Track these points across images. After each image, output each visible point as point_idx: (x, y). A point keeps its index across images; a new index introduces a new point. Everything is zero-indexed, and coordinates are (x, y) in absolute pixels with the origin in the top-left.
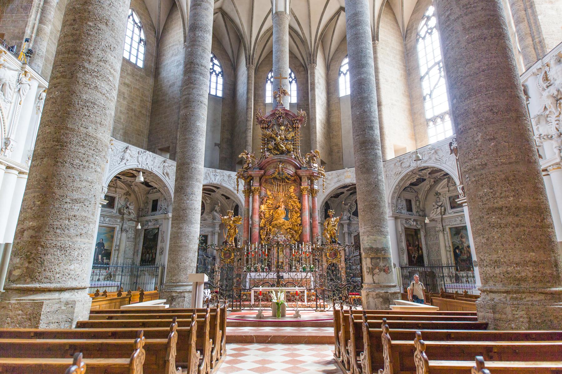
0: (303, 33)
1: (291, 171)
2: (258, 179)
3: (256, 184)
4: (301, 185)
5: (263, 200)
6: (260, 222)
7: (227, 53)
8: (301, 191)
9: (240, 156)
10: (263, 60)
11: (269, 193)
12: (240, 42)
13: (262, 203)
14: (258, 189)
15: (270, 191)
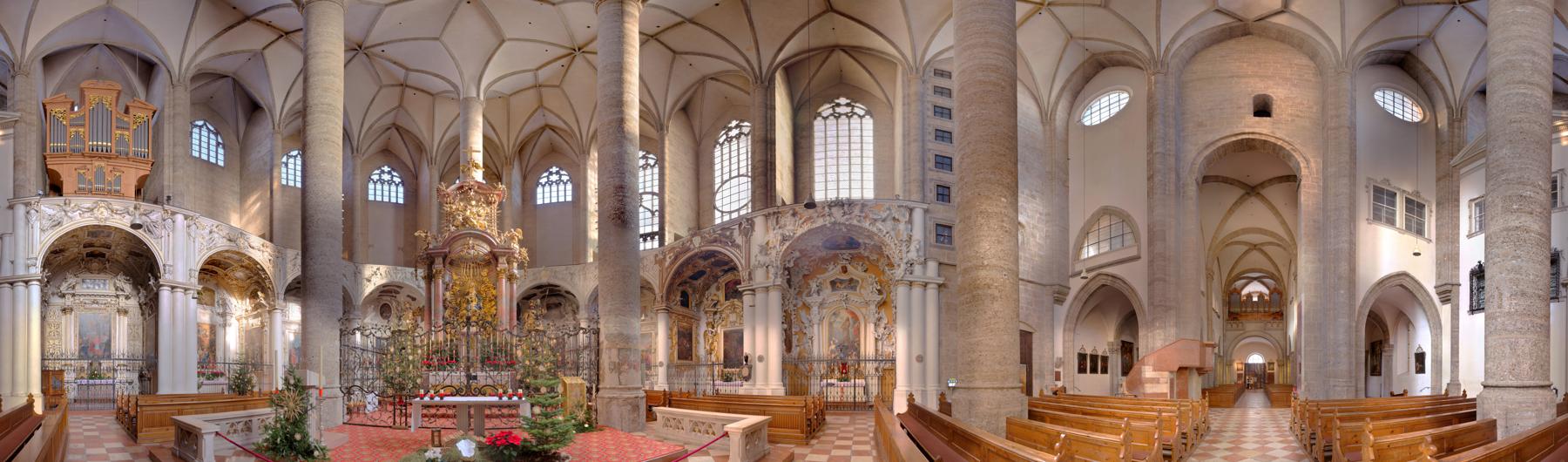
0: (499, 139)
1: (484, 249)
2: (441, 259)
3: (438, 265)
4: (497, 266)
5: (448, 285)
6: (444, 312)
7: (404, 163)
8: (498, 274)
9: (416, 234)
10: (449, 170)
11: (455, 277)
12: (421, 151)
13: (446, 289)
14: (440, 271)
15: (457, 274)
